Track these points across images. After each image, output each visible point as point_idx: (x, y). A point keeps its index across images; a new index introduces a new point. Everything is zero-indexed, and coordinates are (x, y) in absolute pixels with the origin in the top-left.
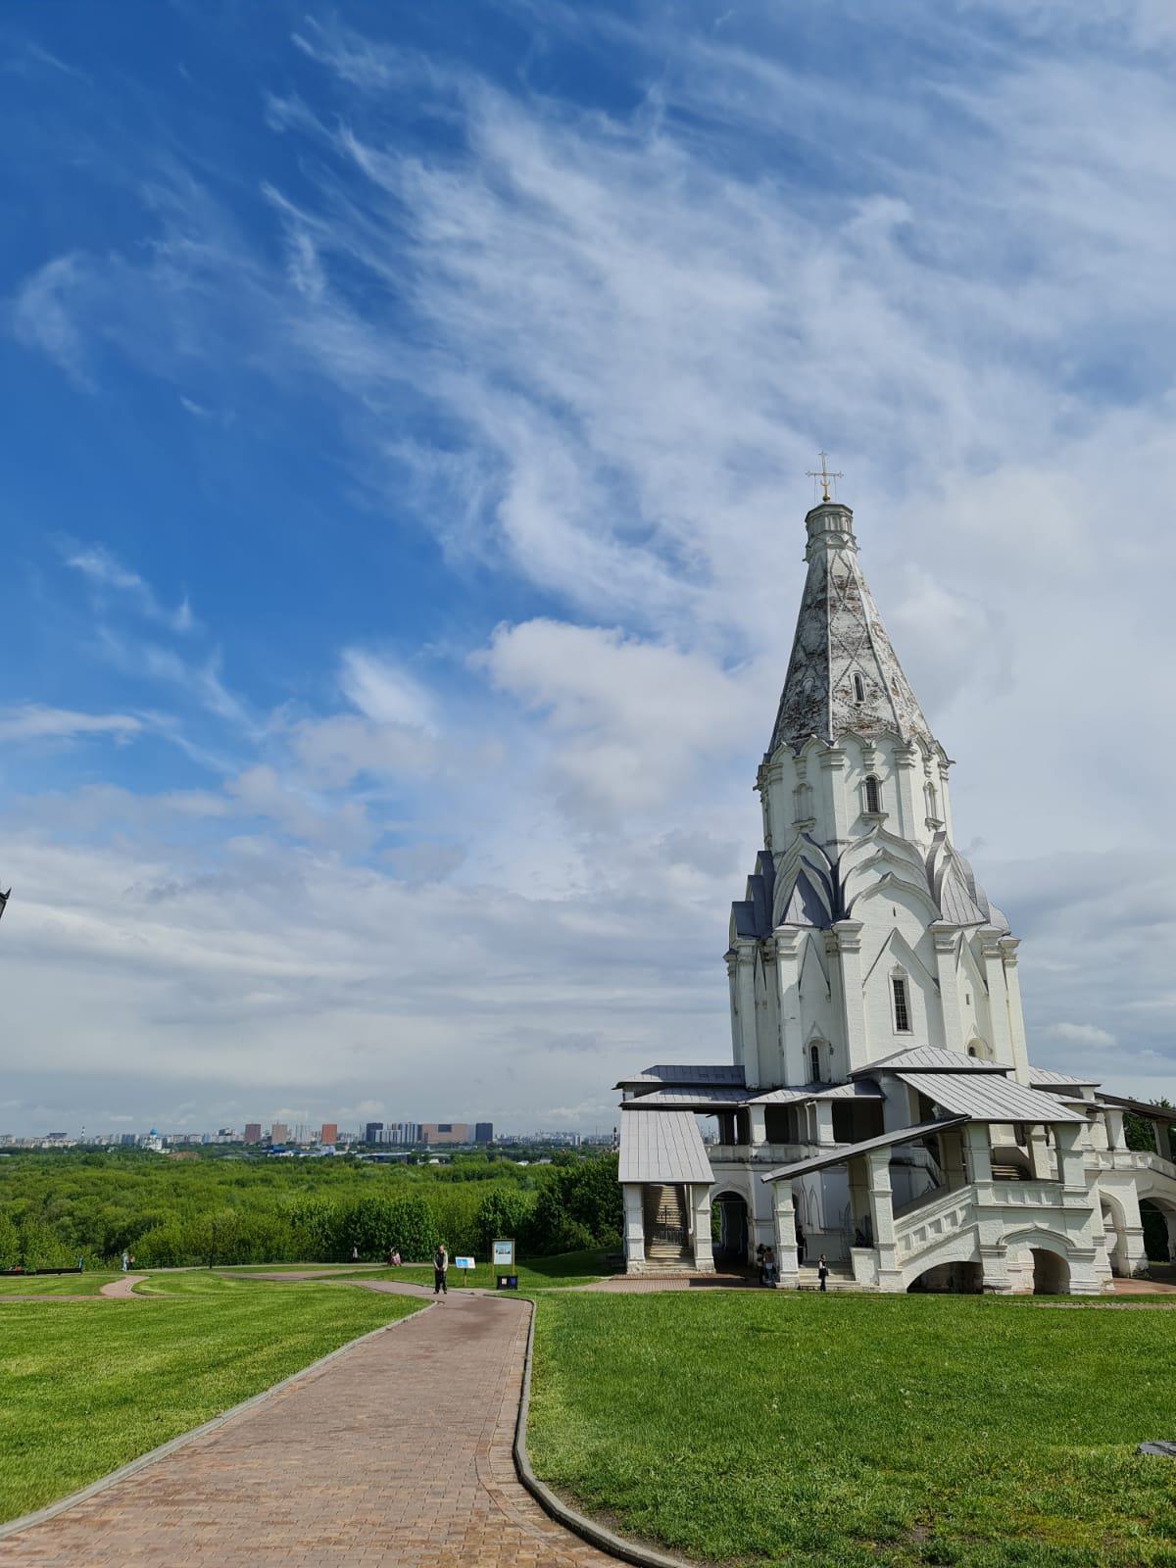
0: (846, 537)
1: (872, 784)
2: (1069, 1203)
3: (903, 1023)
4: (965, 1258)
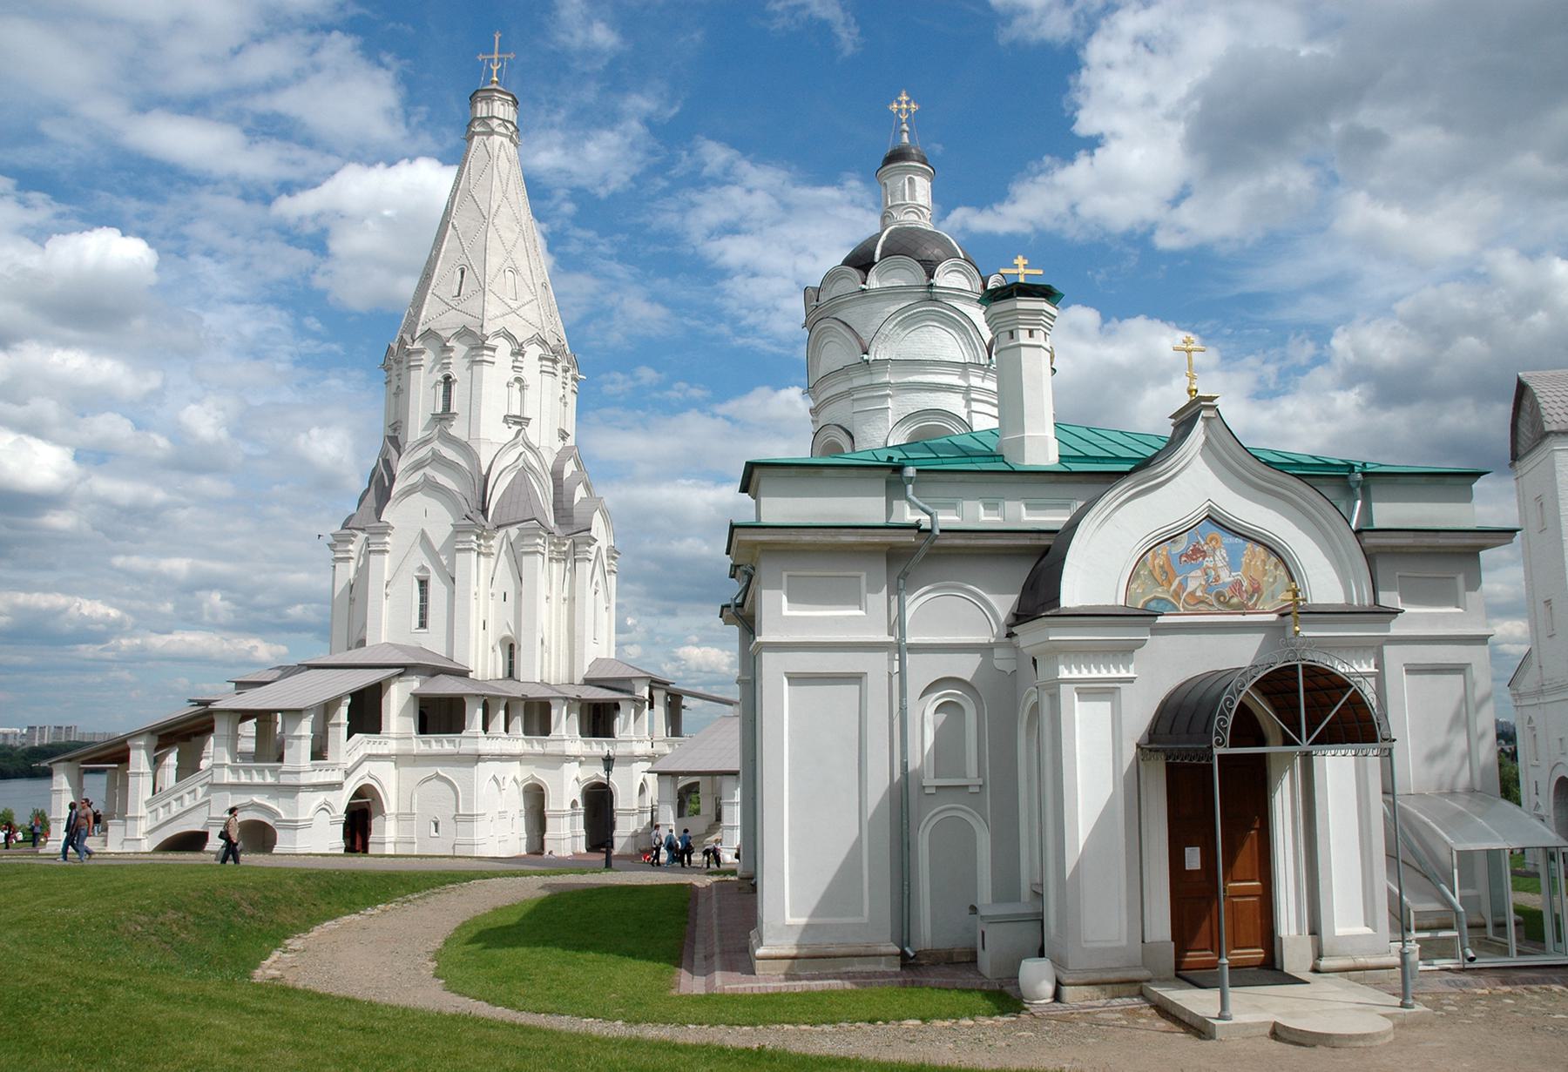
0: (494, 123)
1: (448, 381)
2: (285, 779)
3: (423, 625)
4: (199, 829)
